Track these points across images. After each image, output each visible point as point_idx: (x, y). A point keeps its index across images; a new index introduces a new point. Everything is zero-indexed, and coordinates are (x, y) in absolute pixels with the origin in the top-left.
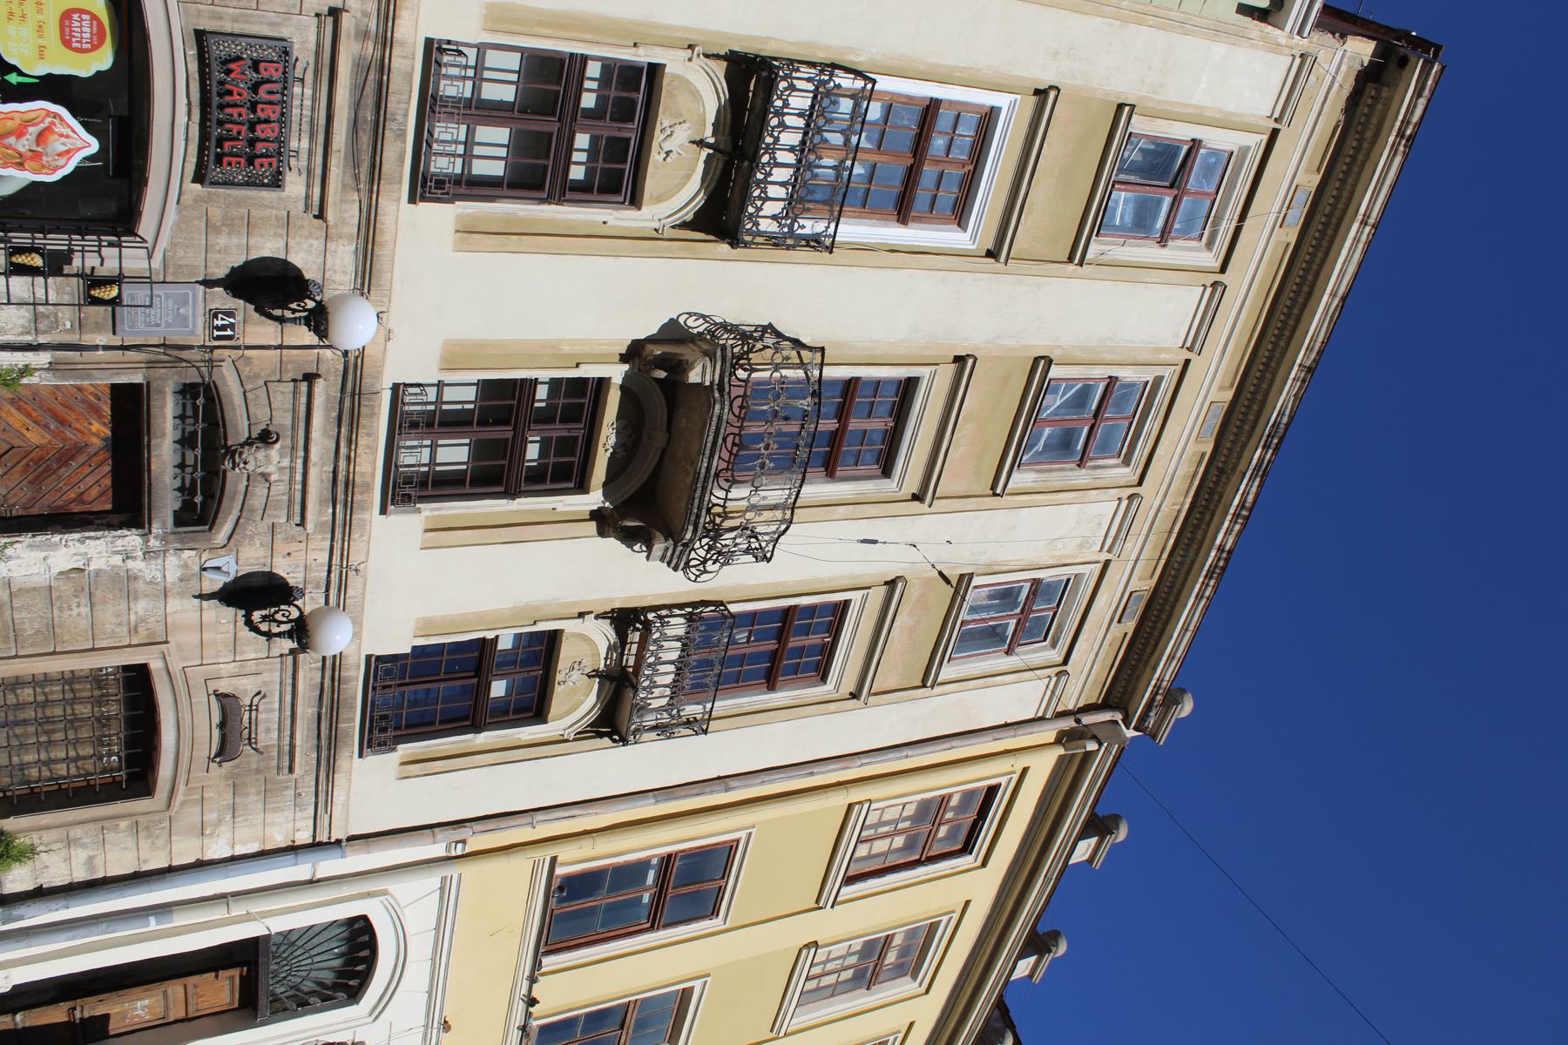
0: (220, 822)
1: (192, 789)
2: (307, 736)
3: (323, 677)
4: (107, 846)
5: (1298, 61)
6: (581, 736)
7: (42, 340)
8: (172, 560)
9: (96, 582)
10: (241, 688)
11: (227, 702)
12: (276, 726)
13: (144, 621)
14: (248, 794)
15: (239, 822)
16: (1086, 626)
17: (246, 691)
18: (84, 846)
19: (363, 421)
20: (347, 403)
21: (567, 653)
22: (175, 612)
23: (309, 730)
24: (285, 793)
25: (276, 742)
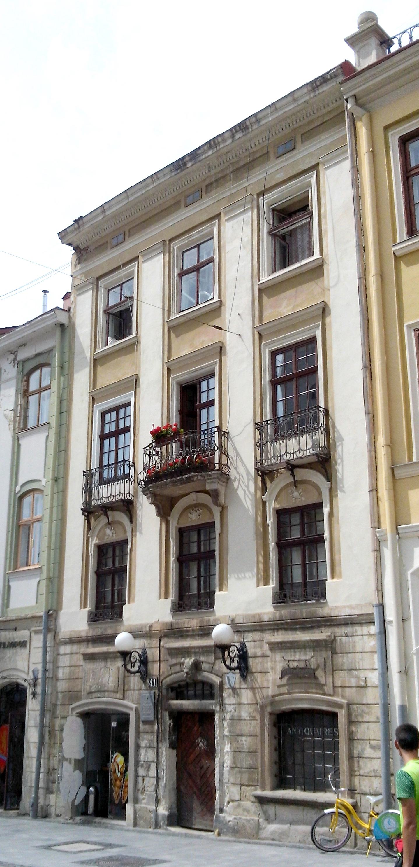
0: (358, 677)
1: (334, 691)
3: (281, 629)
4: (365, 738)
6: (328, 478)
7: (156, 746)
8: (226, 701)
9: (233, 733)
13: (250, 714)
15: (359, 666)
16: (295, 172)
17: (283, 666)
18: (363, 750)
19: (180, 626)
22: (247, 699)
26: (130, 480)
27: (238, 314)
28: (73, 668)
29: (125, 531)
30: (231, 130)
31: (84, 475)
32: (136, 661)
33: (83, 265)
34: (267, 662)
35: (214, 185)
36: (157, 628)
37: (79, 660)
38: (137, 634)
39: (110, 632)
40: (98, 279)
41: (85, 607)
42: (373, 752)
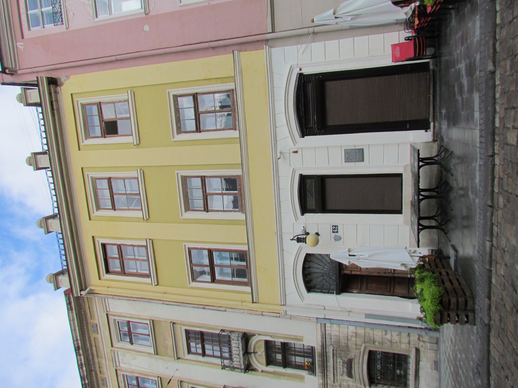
0: (352, 336)
1: (358, 349)
2: (329, 357)
3: (327, 373)
4: (381, 337)
10: (347, 377)
11: (350, 375)
12: (338, 363)
14: (345, 343)
18: (387, 339)
21: (264, 360)
23: (329, 359)
24: (334, 341)
25: (338, 358)
27: (167, 368)
30: (77, 355)
34: (344, 384)
35: (101, 369)
42: (388, 334)
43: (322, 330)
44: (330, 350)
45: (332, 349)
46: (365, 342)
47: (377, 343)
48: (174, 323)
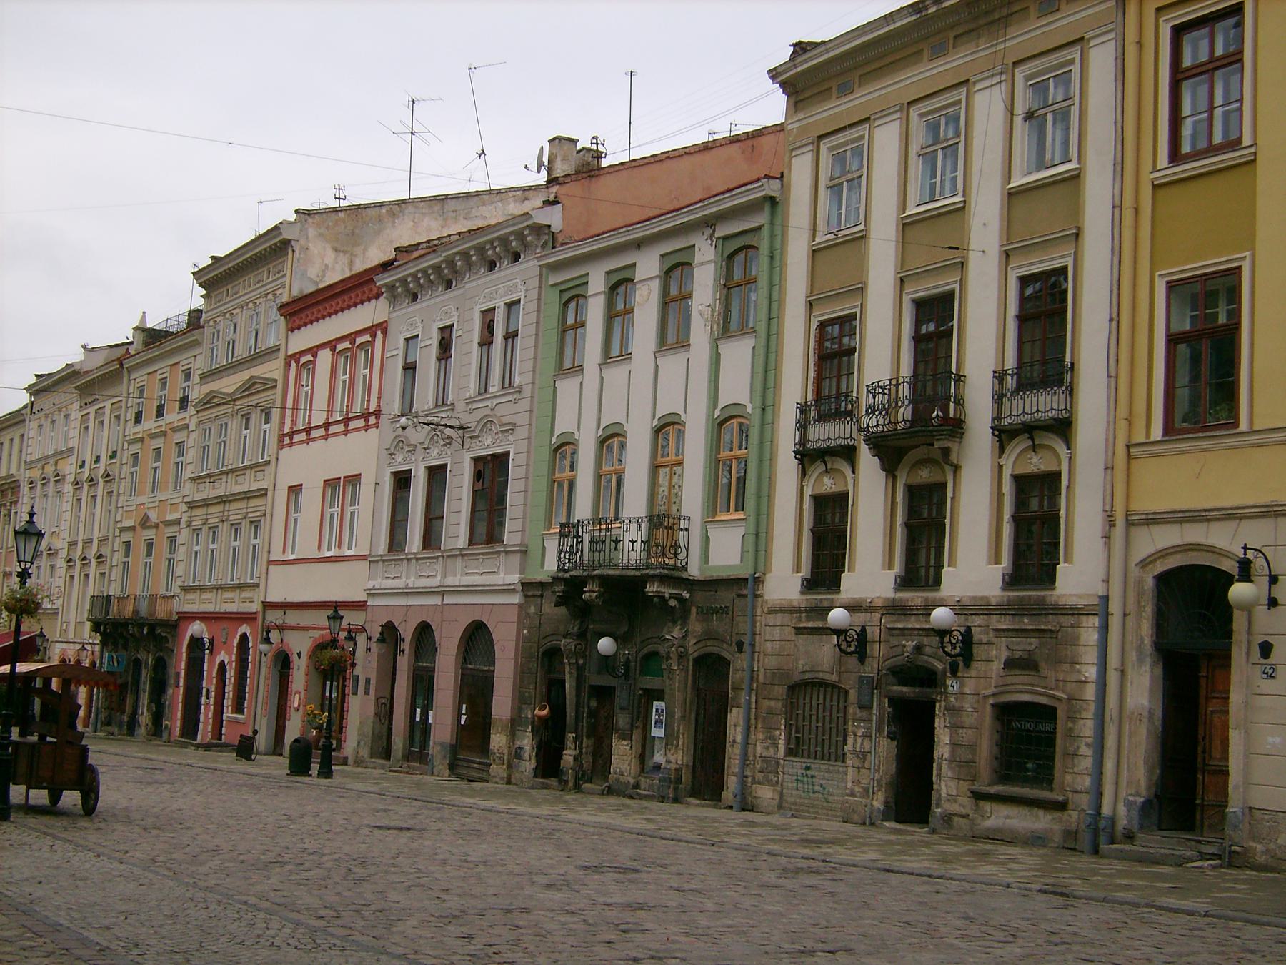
0: (1079, 672)
5: (794, 154)
6: (1068, 445)
11: (1010, 664)
18: (1078, 747)
20: (899, 612)
21: (1021, 471)
25: (1037, 640)
26: (852, 420)
27: (984, 224)
28: (784, 643)
29: (846, 482)
31: (797, 408)
32: (853, 641)
33: (801, 116)
34: (992, 650)
36: (879, 603)
37: (789, 632)
38: (853, 608)
39: (826, 604)
40: (821, 137)
41: (798, 572)
42: (1087, 749)
43: (1086, 608)
44: (1049, 623)
45: (1053, 629)
46: (1070, 699)
47: (1070, 725)
48: (1077, 235)
